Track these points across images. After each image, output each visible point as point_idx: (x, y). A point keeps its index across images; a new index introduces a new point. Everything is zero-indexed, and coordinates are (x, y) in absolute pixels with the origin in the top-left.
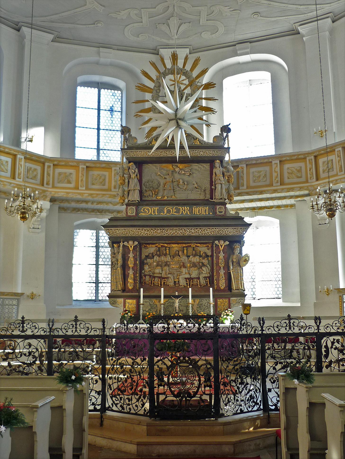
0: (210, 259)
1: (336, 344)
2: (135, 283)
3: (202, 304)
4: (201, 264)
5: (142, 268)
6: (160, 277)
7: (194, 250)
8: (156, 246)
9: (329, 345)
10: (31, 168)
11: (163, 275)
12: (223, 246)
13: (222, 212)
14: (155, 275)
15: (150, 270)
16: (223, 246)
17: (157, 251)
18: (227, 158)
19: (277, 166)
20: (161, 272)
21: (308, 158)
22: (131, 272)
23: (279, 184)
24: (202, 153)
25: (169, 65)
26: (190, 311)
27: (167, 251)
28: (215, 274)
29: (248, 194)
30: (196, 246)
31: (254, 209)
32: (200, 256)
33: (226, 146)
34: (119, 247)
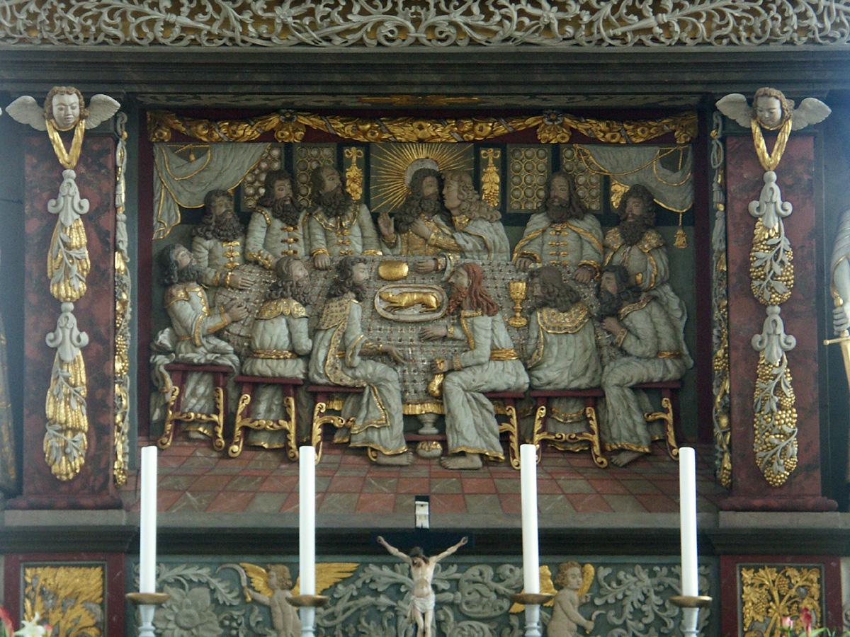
2: (100, 431)
3: (619, 605)
4: (610, 284)
5: (155, 311)
6: (285, 386)
7: (556, 165)
8: (268, 137)
11: (327, 368)
12: (784, 137)
14: (262, 367)
15: (217, 322)
16: (784, 137)
17: (272, 176)
20: (305, 343)
27: (353, 172)
28: (718, 365)
30: (576, 137)
32: (608, 218)
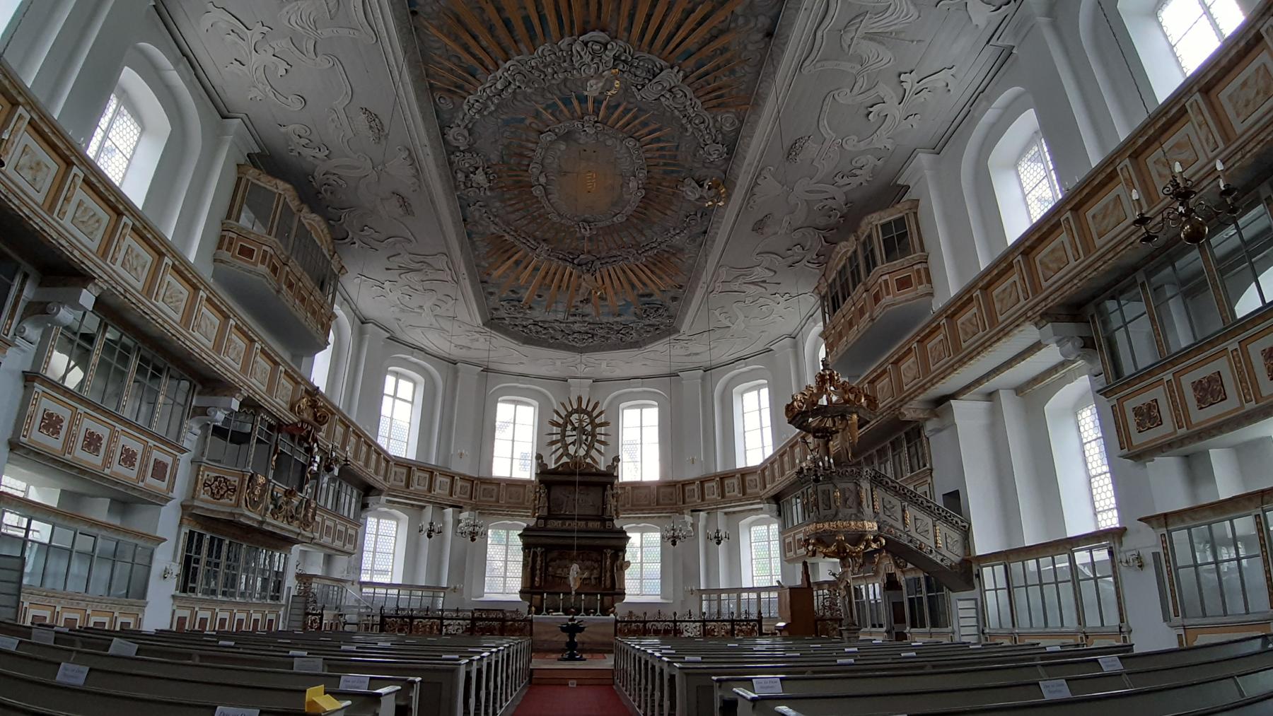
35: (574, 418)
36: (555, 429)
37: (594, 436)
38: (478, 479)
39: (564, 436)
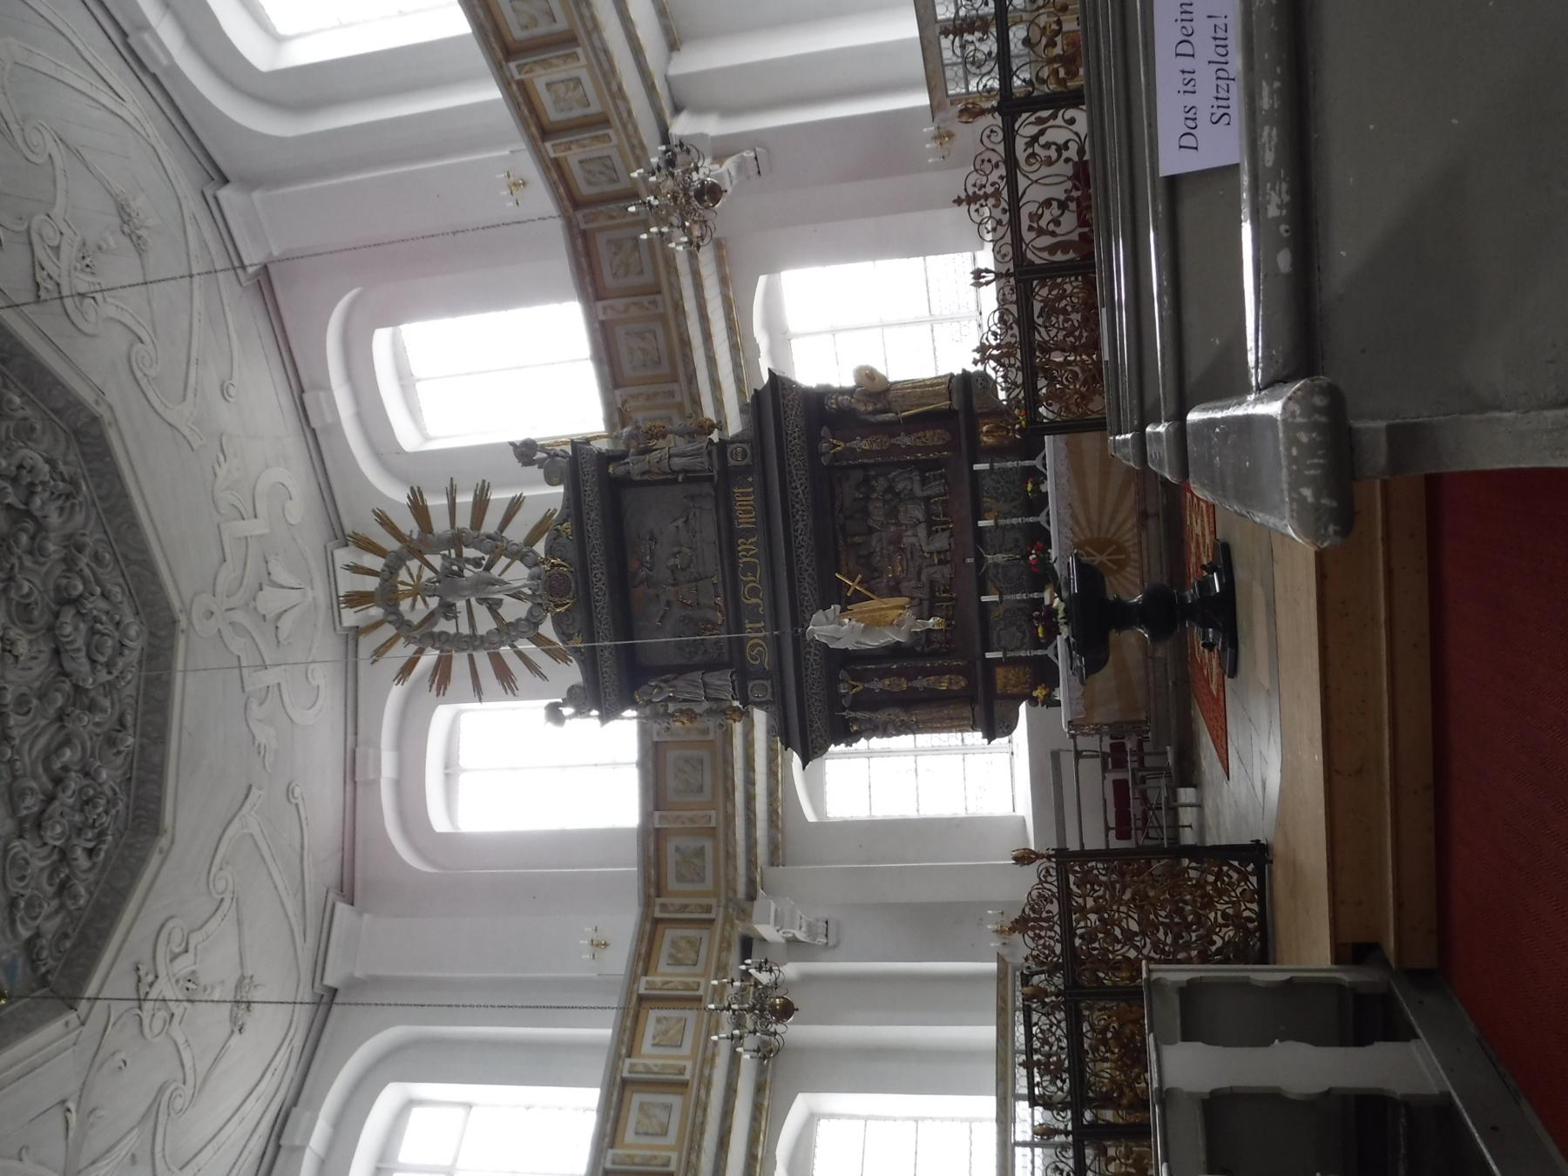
0: (873, 473)
1: (1043, 223)
4: (888, 496)
9: (1046, 241)
10: (671, 956)
13: (744, 451)
18: (603, 445)
19: (612, 308)
21: (583, 226)
22: (921, 683)
23: (658, 297)
24: (593, 515)
25: (376, 612)
26: (1014, 521)
29: (692, 378)
31: (735, 348)
32: (867, 498)
33: (568, 449)
34: (856, 719)
35: (415, 610)
36: (460, 662)
37: (457, 540)
38: (647, 903)
39: (472, 642)
